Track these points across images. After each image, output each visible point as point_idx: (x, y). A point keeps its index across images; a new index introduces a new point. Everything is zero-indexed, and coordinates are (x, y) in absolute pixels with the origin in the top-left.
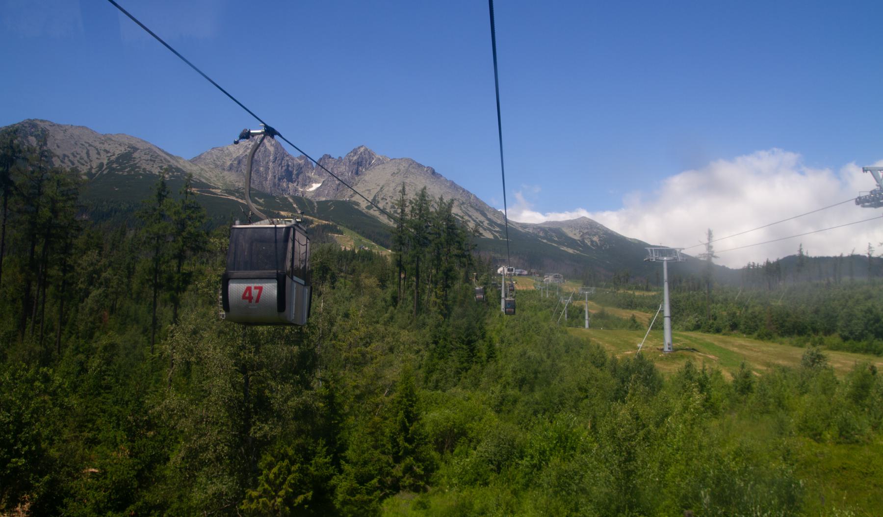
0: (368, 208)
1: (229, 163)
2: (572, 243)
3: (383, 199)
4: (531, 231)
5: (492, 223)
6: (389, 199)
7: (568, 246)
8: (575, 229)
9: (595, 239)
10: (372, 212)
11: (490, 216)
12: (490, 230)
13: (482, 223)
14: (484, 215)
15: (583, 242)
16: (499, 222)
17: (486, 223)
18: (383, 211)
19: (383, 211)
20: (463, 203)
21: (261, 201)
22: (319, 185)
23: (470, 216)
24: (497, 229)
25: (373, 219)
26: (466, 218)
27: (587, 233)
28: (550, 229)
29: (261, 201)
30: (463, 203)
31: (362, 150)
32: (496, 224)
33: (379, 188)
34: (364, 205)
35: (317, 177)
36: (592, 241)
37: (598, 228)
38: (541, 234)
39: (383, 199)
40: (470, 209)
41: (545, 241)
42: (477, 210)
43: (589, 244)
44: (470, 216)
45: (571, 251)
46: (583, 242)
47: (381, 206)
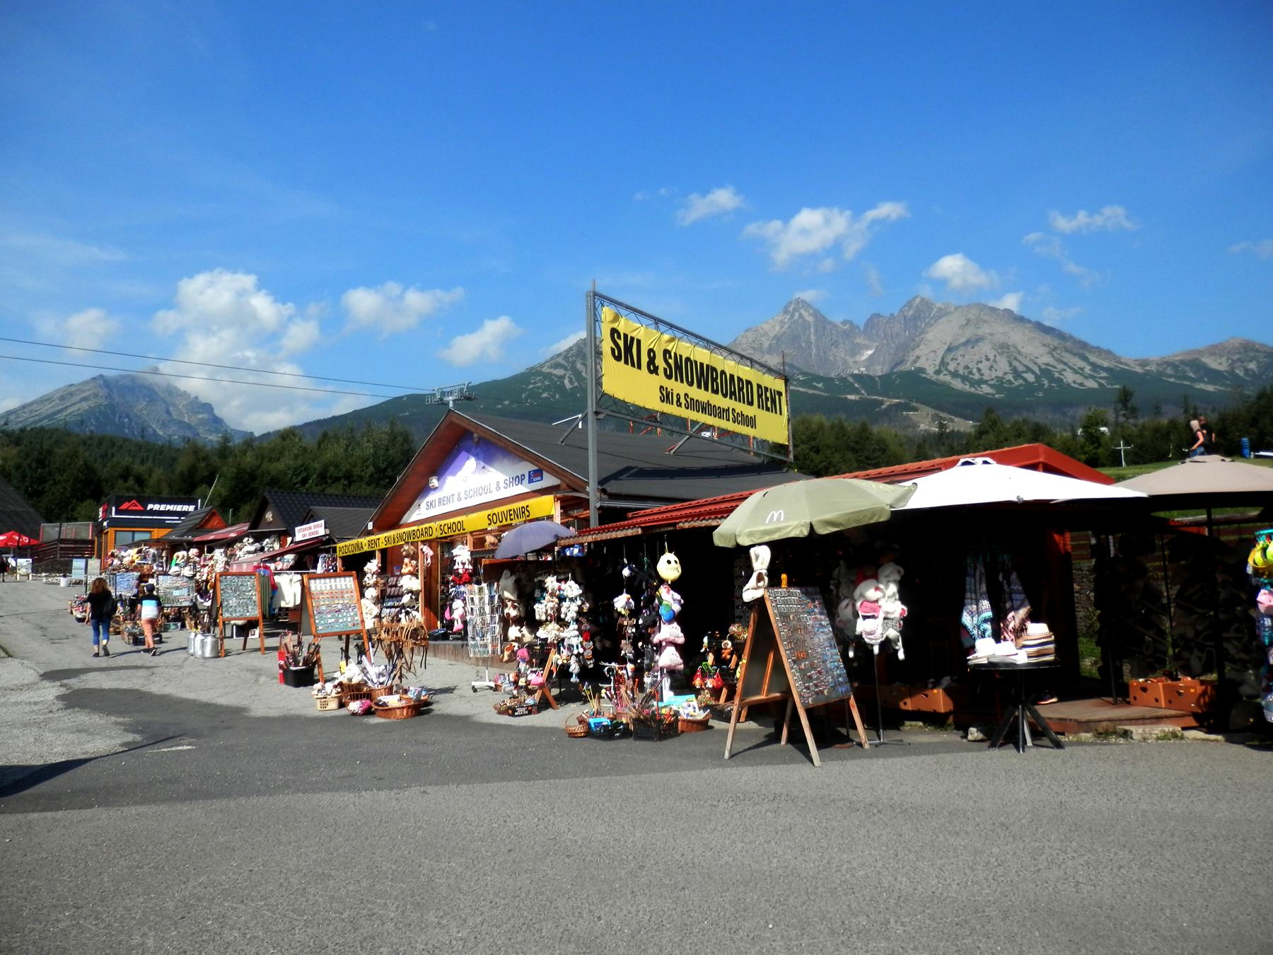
0: (938, 372)
1: (766, 344)
2: (1214, 376)
5: (1095, 367)
7: (1206, 383)
8: (1221, 356)
9: (1252, 366)
10: (942, 377)
11: (1092, 358)
12: (1092, 377)
13: (1082, 369)
14: (1085, 359)
15: (1232, 372)
16: (1106, 364)
17: (1088, 369)
18: (955, 375)
19: (955, 375)
20: (1055, 349)
21: (820, 385)
22: (870, 352)
23: (1065, 364)
24: (1104, 374)
25: (945, 387)
26: (1061, 366)
27: (1239, 360)
28: (1182, 362)
29: (820, 385)
30: (1055, 349)
31: (918, 300)
34: (930, 371)
35: (866, 342)
36: (1246, 370)
37: (1257, 351)
38: (1169, 371)
40: (1064, 354)
41: (1172, 380)
42: (1075, 354)
44: (1065, 364)
45: (1210, 388)
46: (1232, 372)
47: (951, 367)
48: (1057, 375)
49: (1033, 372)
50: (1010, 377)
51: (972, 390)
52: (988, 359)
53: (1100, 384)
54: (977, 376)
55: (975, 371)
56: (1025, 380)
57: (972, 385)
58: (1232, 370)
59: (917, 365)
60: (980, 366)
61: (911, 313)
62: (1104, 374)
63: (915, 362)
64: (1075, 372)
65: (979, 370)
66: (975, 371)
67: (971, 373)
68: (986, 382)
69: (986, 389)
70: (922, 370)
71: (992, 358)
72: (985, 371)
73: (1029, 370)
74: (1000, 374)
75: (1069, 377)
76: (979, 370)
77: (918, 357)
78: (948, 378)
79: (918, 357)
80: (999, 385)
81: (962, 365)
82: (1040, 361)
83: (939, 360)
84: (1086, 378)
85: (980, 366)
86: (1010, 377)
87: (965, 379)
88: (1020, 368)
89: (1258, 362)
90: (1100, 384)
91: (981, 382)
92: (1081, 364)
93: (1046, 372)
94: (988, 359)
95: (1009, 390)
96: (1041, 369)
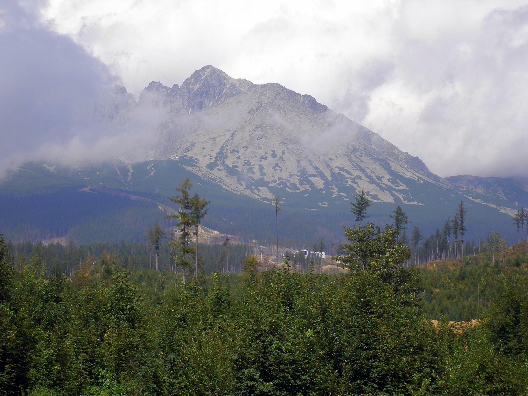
0: (211, 166)
3: (233, 151)
6: (242, 151)
11: (395, 167)
16: (408, 175)
19: (232, 171)
24: (403, 187)
33: (228, 135)
39: (233, 151)
41: (478, 201)
47: (229, 162)
49: (323, 177)
50: (295, 180)
51: (248, 192)
52: (274, 156)
54: (257, 176)
55: (256, 168)
56: (312, 185)
60: (264, 163)
61: (197, 86)
62: (403, 187)
63: (188, 149)
65: (261, 168)
66: (256, 168)
68: (265, 184)
69: (264, 193)
70: (192, 162)
71: (279, 153)
72: (269, 170)
73: (320, 174)
74: (284, 175)
76: (261, 168)
77: (193, 145)
82: (334, 164)
83: (217, 150)
84: (382, 189)
85: (264, 163)
86: (295, 180)
88: (310, 170)
94: (274, 156)
96: (333, 174)
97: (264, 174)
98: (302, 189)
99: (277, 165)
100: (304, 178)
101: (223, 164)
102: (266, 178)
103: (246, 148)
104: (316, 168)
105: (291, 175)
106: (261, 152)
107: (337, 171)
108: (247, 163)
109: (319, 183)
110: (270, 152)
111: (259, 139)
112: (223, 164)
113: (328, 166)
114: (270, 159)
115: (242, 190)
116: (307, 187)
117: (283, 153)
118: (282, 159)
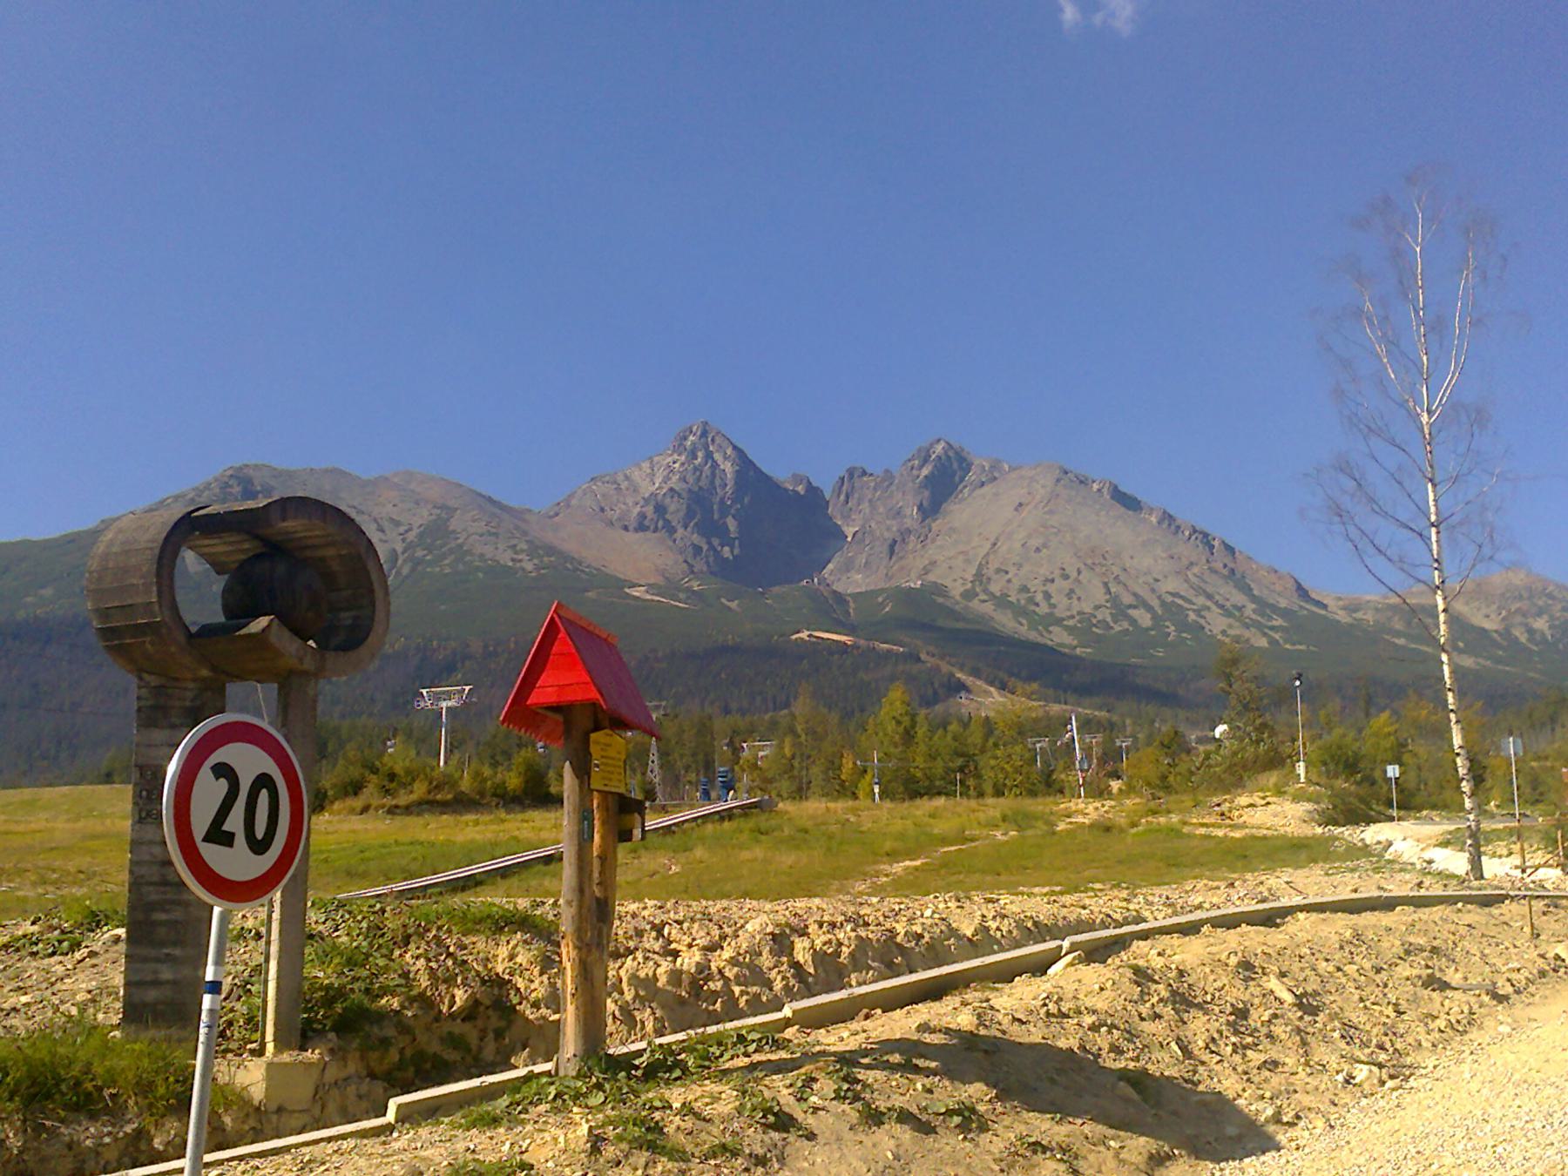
0: (969, 595)
3: (998, 571)
4: (1370, 617)
5: (1263, 606)
6: (1012, 570)
9: (1541, 624)
12: (1259, 626)
13: (1240, 609)
14: (1246, 590)
15: (1506, 633)
19: (1002, 601)
24: (1279, 622)
26: (1201, 601)
31: (939, 448)
32: (1275, 609)
34: (956, 590)
36: (1531, 631)
37: (1550, 596)
38: (1398, 625)
40: (1207, 577)
41: (1401, 641)
43: (1523, 639)
44: (1209, 597)
47: (995, 588)
48: (1192, 616)
49: (1149, 608)
50: (1105, 614)
51: (1033, 636)
52: (1066, 577)
53: (1273, 642)
54: (1043, 609)
56: (1133, 622)
57: (1033, 626)
58: (1507, 630)
59: (931, 577)
60: (1051, 588)
62: (1279, 622)
63: (926, 571)
64: (1227, 613)
65: (1047, 596)
66: (1039, 598)
67: (1031, 600)
70: (941, 590)
72: (1060, 601)
73: (1143, 603)
75: (1217, 623)
76: (1047, 596)
77: (933, 563)
78: (988, 608)
79: (933, 563)
80: (1085, 628)
81: (1016, 583)
85: (1051, 588)
86: (1105, 614)
87: (1020, 612)
88: (1127, 599)
89: (1552, 618)
90: (1273, 642)
91: (1052, 620)
92: (1238, 598)
93: (1172, 610)
94: (1066, 577)
95: (1098, 639)
96: (1163, 604)
97: (1054, 606)
98: (1117, 628)
99: (1072, 591)
100: (1120, 611)
101: (985, 591)
102: (1059, 613)
103: (1019, 566)
104: (1135, 595)
105: (1097, 607)
106: (1044, 571)
107: (1169, 599)
108: (1024, 589)
109: (1144, 619)
110: (1057, 572)
111: (1038, 550)
112: (985, 591)
113: (1153, 590)
114: (1059, 583)
115: (1024, 631)
116: (1126, 625)
117: (1079, 572)
118: (1077, 581)
